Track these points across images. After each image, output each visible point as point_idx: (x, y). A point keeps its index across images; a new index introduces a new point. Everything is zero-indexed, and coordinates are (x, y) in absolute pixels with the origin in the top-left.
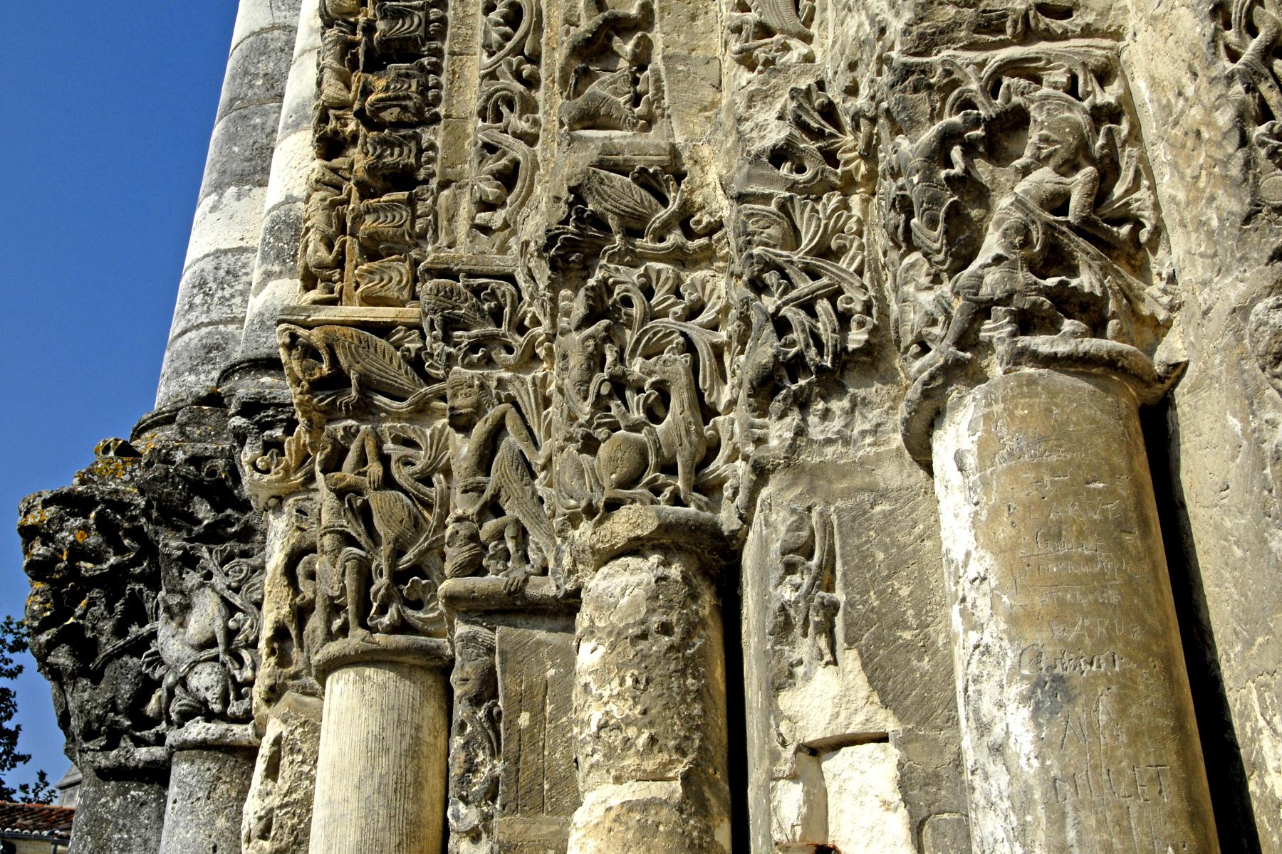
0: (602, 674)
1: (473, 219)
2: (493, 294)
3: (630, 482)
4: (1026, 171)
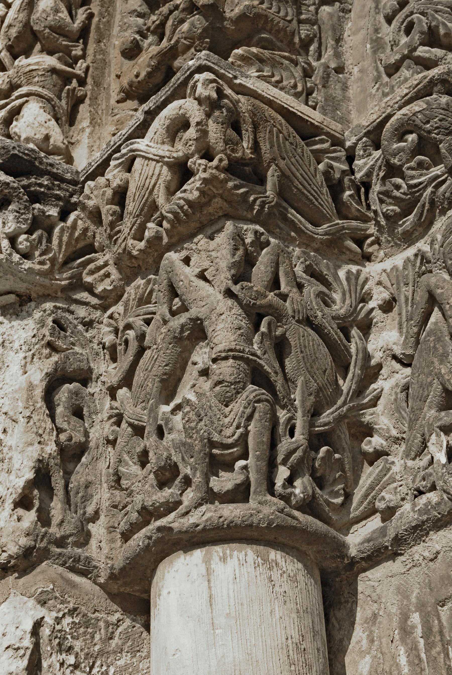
1: (415, 49)
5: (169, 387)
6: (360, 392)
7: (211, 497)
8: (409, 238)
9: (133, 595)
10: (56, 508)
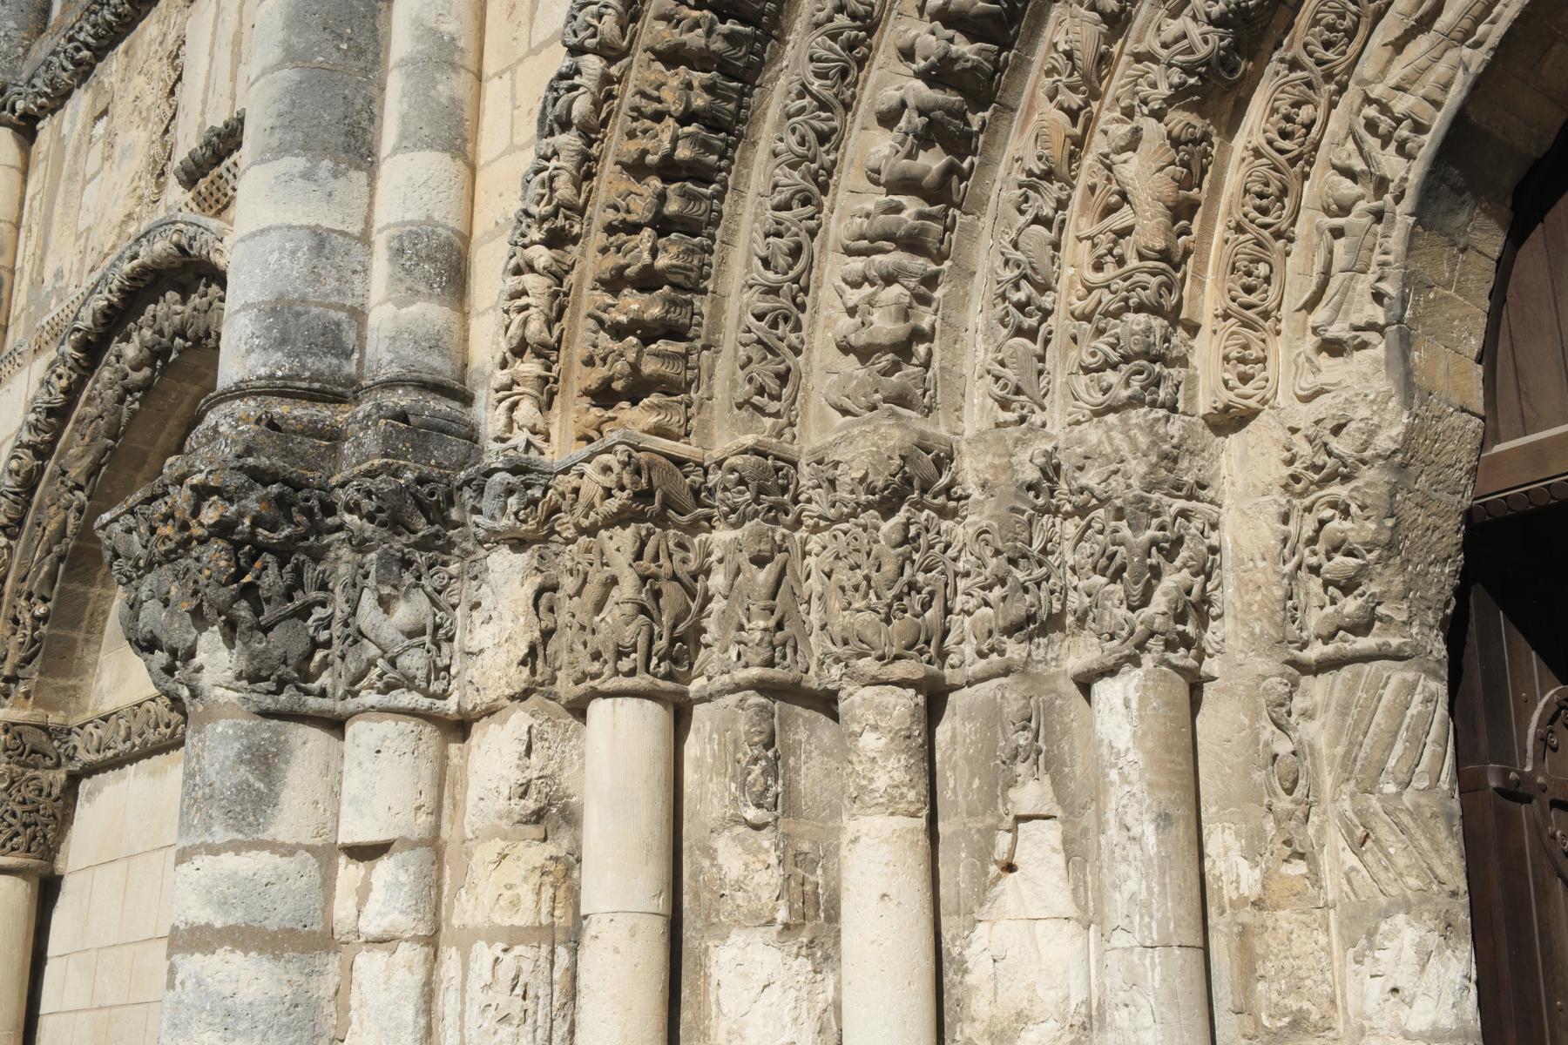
0: (887, 754)
2: (786, 476)
3: (910, 647)
4: (1180, 570)
5: (599, 607)
6: (702, 608)
7: (617, 672)
8: (735, 526)
9: (578, 709)
10: (540, 663)
